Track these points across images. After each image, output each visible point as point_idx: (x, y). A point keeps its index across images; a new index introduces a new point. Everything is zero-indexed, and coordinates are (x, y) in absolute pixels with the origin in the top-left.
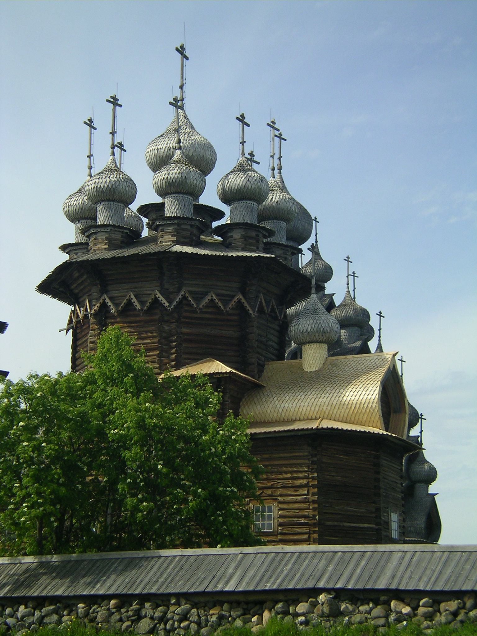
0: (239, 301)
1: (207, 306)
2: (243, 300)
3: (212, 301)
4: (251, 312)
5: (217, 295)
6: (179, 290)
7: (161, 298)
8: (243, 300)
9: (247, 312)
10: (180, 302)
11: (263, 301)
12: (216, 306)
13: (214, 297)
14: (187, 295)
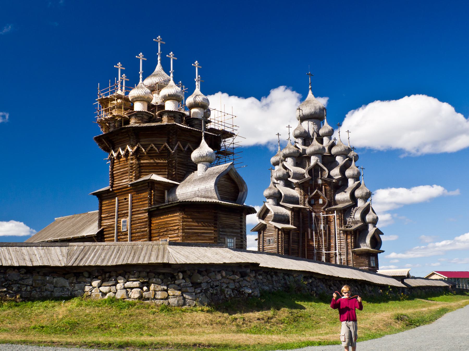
5: (155, 145)
6: (137, 144)
8: (167, 146)
13: (153, 146)
14: (140, 146)
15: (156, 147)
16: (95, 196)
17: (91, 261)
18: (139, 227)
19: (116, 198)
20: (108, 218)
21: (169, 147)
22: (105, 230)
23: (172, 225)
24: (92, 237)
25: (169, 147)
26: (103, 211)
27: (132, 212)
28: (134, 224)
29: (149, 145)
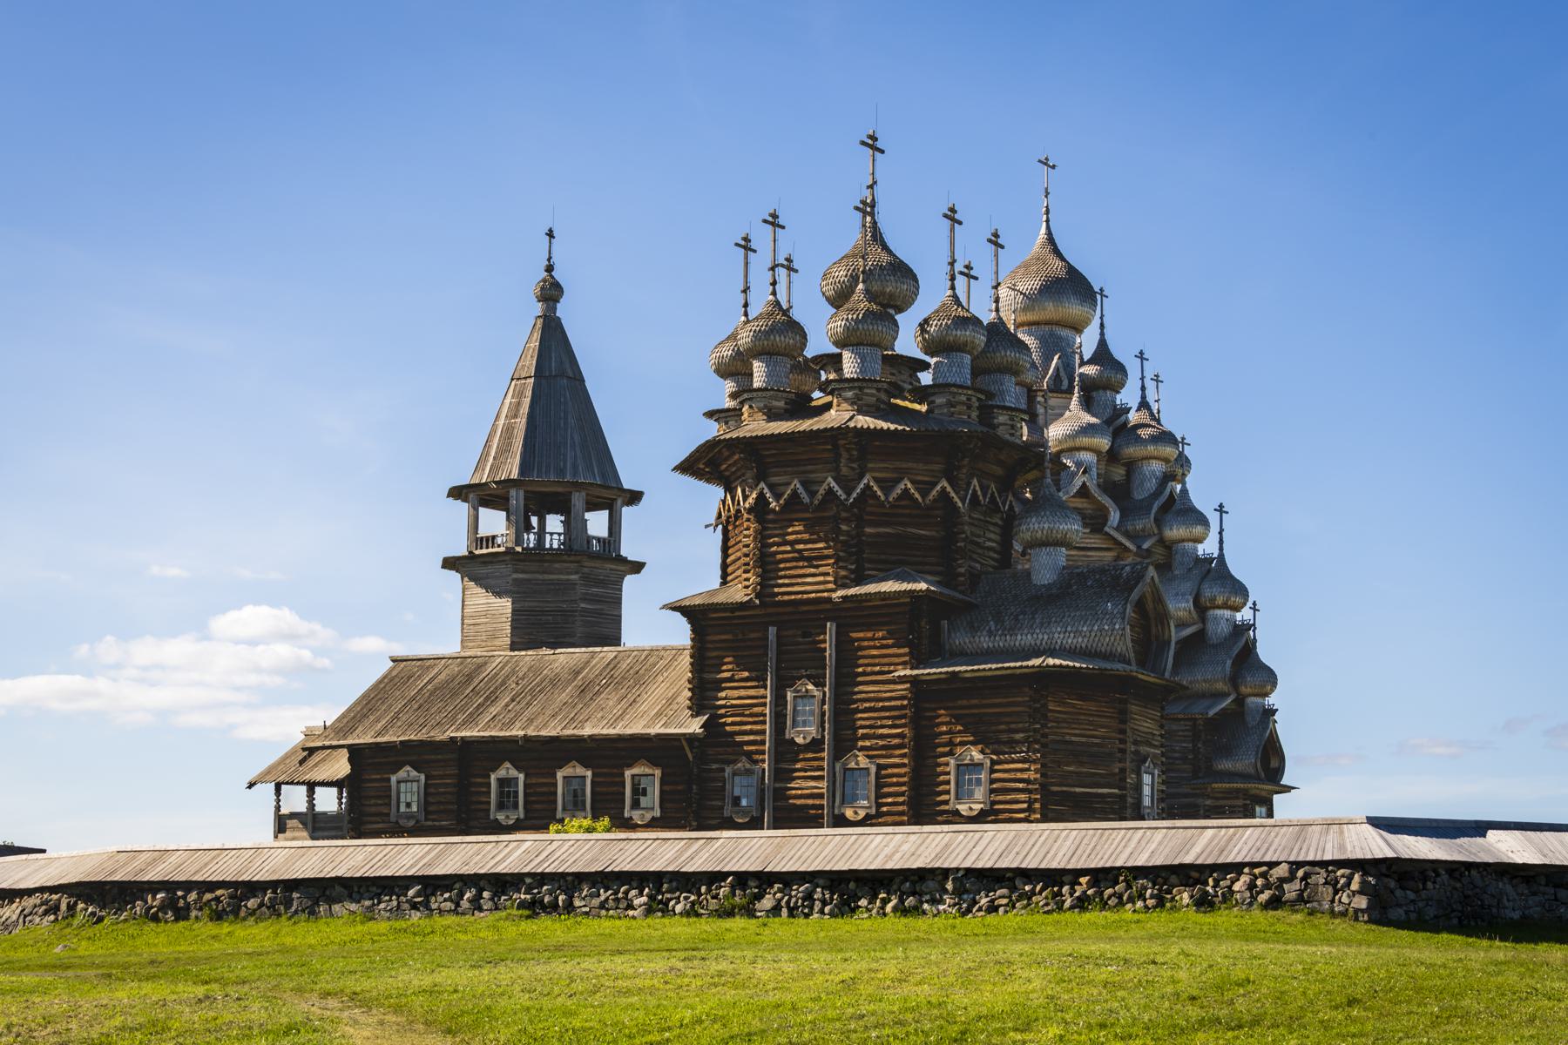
0: (944, 489)
1: (900, 498)
2: (949, 489)
3: (906, 490)
4: (960, 504)
5: (912, 482)
6: (861, 477)
7: (836, 488)
8: (949, 489)
10: (863, 491)
11: (978, 488)
13: (909, 486)
14: (872, 484)
15: (916, 489)
16: (678, 614)
21: (953, 494)
25: (953, 494)
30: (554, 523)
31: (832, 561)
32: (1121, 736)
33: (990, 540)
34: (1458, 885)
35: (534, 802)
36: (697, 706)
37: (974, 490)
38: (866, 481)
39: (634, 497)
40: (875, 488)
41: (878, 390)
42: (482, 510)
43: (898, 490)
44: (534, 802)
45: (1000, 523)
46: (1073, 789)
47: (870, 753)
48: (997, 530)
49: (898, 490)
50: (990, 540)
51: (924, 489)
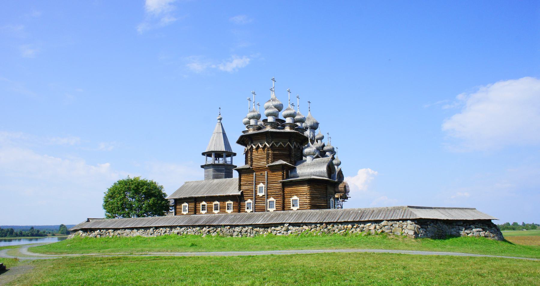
0: (288, 144)
1: (279, 146)
2: (290, 144)
3: (281, 144)
4: (292, 147)
5: (282, 143)
6: (272, 141)
8: (290, 144)
9: (291, 147)
10: (272, 145)
12: (282, 146)
17: (381, 217)
18: (274, 191)
19: (254, 173)
20: (247, 185)
21: (290, 145)
22: (244, 192)
23: (301, 192)
24: (236, 196)
25: (290, 145)
26: (242, 180)
27: (267, 182)
28: (269, 189)
29: (279, 142)
30: (220, 159)
31: (266, 159)
32: (326, 193)
33: (298, 155)
34: (436, 226)
35: (208, 209)
36: (240, 189)
37: (295, 144)
38: (272, 142)
39: (235, 154)
40: (275, 144)
41: (275, 124)
42: (208, 157)
43: (279, 144)
44: (208, 209)
45: (300, 151)
46: (316, 204)
47: (275, 198)
48: (300, 153)
49: (279, 144)
50: (298, 155)
51: (285, 144)
